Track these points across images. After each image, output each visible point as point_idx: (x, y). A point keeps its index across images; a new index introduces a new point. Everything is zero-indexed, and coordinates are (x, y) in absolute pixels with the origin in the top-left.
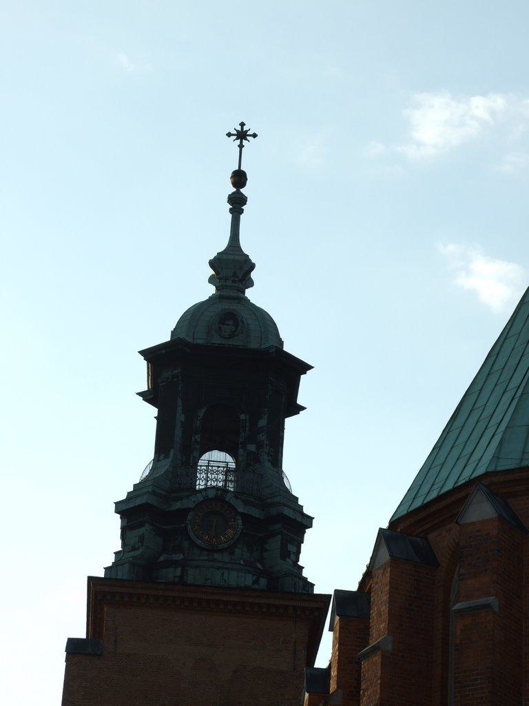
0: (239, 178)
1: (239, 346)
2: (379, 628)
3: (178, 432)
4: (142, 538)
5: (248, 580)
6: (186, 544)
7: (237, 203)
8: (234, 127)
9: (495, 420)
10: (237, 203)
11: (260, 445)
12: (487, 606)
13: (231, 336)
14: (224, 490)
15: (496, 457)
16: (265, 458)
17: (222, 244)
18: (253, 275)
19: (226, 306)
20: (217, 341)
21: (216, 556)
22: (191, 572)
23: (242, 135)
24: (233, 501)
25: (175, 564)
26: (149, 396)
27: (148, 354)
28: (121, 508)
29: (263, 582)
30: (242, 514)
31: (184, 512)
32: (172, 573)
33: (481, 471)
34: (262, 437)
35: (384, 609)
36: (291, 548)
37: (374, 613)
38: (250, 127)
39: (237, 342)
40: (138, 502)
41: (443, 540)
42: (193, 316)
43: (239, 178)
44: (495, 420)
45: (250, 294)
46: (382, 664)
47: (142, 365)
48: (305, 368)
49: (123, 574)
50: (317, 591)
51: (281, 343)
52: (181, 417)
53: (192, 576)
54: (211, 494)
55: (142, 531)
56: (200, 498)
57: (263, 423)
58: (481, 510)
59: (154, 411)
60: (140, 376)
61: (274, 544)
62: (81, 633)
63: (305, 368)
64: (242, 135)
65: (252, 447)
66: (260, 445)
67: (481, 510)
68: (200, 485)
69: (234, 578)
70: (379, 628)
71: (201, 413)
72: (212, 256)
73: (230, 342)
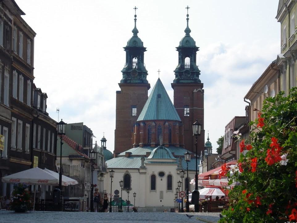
0: (135, 16)
1: (136, 46)
3: (129, 59)
4: (125, 76)
5: (139, 81)
7: (135, 20)
8: (134, 7)
10: (135, 20)
13: (135, 44)
16: (141, 63)
20: (133, 45)
21: (135, 78)
22: (132, 81)
23: (135, 9)
25: (129, 80)
27: (124, 48)
28: (122, 71)
29: (141, 81)
30: (138, 72)
31: (130, 72)
32: (129, 81)
34: (140, 59)
36: (145, 76)
39: (136, 45)
43: (135, 16)
45: (138, 34)
48: (146, 48)
51: (142, 43)
52: (129, 57)
53: (132, 82)
54: (133, 69)
55: (125, 75)
56: (132, 70)
57: (140, 57)
58: (142, 124)
61: (143, 75)
64: (135, 9)
66: (140, 61)
69: (137, 81)
71: (132, 56)
72: (132, 30)
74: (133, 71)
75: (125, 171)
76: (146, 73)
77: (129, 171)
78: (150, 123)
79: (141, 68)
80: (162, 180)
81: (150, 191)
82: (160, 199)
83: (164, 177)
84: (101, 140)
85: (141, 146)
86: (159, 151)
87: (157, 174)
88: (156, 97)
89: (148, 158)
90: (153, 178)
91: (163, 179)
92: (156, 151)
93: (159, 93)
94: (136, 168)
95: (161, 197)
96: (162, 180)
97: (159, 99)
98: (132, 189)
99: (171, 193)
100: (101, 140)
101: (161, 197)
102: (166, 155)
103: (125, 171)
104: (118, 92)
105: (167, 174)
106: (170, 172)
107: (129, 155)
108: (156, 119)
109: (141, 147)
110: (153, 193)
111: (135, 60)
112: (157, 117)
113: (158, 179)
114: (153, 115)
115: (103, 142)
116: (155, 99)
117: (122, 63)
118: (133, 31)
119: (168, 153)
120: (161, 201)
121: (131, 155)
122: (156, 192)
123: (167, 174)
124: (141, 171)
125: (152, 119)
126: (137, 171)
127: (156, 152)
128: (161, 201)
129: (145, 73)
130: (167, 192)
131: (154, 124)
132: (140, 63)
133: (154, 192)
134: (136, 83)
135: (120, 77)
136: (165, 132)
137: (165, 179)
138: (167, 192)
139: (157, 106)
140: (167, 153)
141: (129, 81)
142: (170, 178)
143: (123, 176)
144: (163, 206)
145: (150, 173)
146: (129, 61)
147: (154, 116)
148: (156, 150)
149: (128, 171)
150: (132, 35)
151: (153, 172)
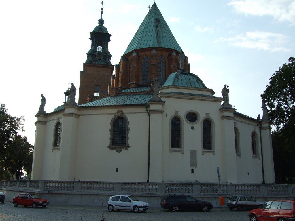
0: (102, 9)
2: (121, 69)
4: (90, 58)
5: (104, 63)
6: (96, 59)
7: (102, 12)
8: (101, 2)
9: (136, 42)
10: (102, 12)
11: (105, 45)
12: (135, 67)
13: (101, 31)
14: (101, 51)
15: (136, 47)
16: (106, 47)
17: (100, 18)
18: (104, 23)
19: (100, 27)
20: (99, 31)
23: (102, 3)
24: (102, 53)
26: (91, 39)
29: (106, 64)
32: (94, 62)
33: (134, 49)
35: (122, 67)
37: (120, 67)
38: (103, 2)
40: (89, 53)
41: (129, 58)
42: (96, 28)
43: (102, 9)
44: (136, 42)
45: (104, 25)
46: (122, 74)
47: (89, 35)
48: (111, 35)
49: (87, 62)
50: (113, 65)
52: (95, 42)
57: (105, 43)
59: (91, 41)
60: (89, 36)
61: (107, 59)
62: (82, 70)
63: (111, 35)
64: (102, 3)
65: (104, 46)
66: (105, 45)
67: (134, 54)
68: (97, 51)
69: (102, 63)
70: (121, 69)
73: (101, 32)
74: (98, 53)
75: (115, 111)
76: (110, 56)
77: (125, 110)
78: (147, 53)
79: (106, 52)
80: (192, 128)
81: (171, 151)
82: (191, 166)
83: (196, 122)
84: (65, 93)
85: (134, 86)
86: (182, 76)
87: (182, 115)
88: (153, 21)
89: (165, 85)
90: (176, 123)
91: (194, 126)
92: (177, 77)
93: (157, 18)
94: (141, 103)
95: (193, 163)
96: (192, 128)
97: (158, 24)
98: (130, 146)
99: (211, 154)
100: (65, 93)
101: (193, 163)
102: (197, 84)
103: (115, 111)
104: (81, 72)
105: (202, 117)
106: (207, 114)
107: (117, 93)
108: (156, 46)
109: (134, 88)
110: (177, 154)
111: (99, 48)
112: (158, 45)
113: (186, 126)
114: (152, 41)
115: (67, 97)
116: (153, 24)
117: (88, 45)
118: (99, 21)
119: (199, 81)
120: (192, 171)
121: (120, 94)
122: (182, 152)
123: (202, 117)
124: (153, 107)
125: (151, 46)
126: (143, 109)
127: (178, 78)
128: (192, 171)
129: (109, 56)
130: (203, 153)
131: (154, 52)
132: (105, 48)
133: (179, 153)
134: (101, 64)
135: (85, 59)
136: (172, 66)
137: (199, 126)
138: (203, 153)
139: (157, 31)
140: (197, 81)
141: (94, 62)
142: (207, 125)
143: (111, 121)
144: (196, 181)
145: (170, 114)
146: (94, 45)
147: (154, 42)
148: (177, 75)
149: (122, 112)
150: (97, 24)
151: (176, 112)
